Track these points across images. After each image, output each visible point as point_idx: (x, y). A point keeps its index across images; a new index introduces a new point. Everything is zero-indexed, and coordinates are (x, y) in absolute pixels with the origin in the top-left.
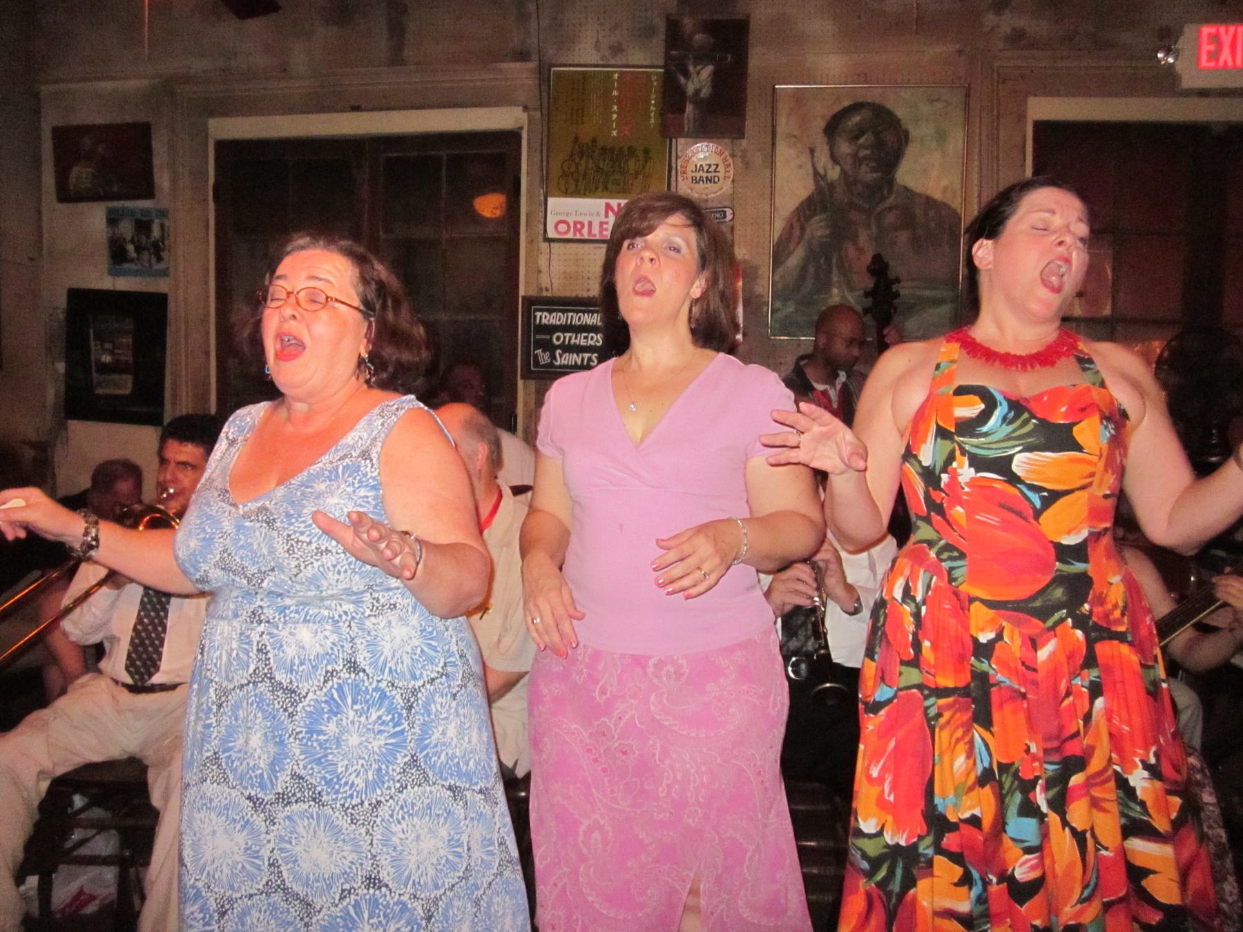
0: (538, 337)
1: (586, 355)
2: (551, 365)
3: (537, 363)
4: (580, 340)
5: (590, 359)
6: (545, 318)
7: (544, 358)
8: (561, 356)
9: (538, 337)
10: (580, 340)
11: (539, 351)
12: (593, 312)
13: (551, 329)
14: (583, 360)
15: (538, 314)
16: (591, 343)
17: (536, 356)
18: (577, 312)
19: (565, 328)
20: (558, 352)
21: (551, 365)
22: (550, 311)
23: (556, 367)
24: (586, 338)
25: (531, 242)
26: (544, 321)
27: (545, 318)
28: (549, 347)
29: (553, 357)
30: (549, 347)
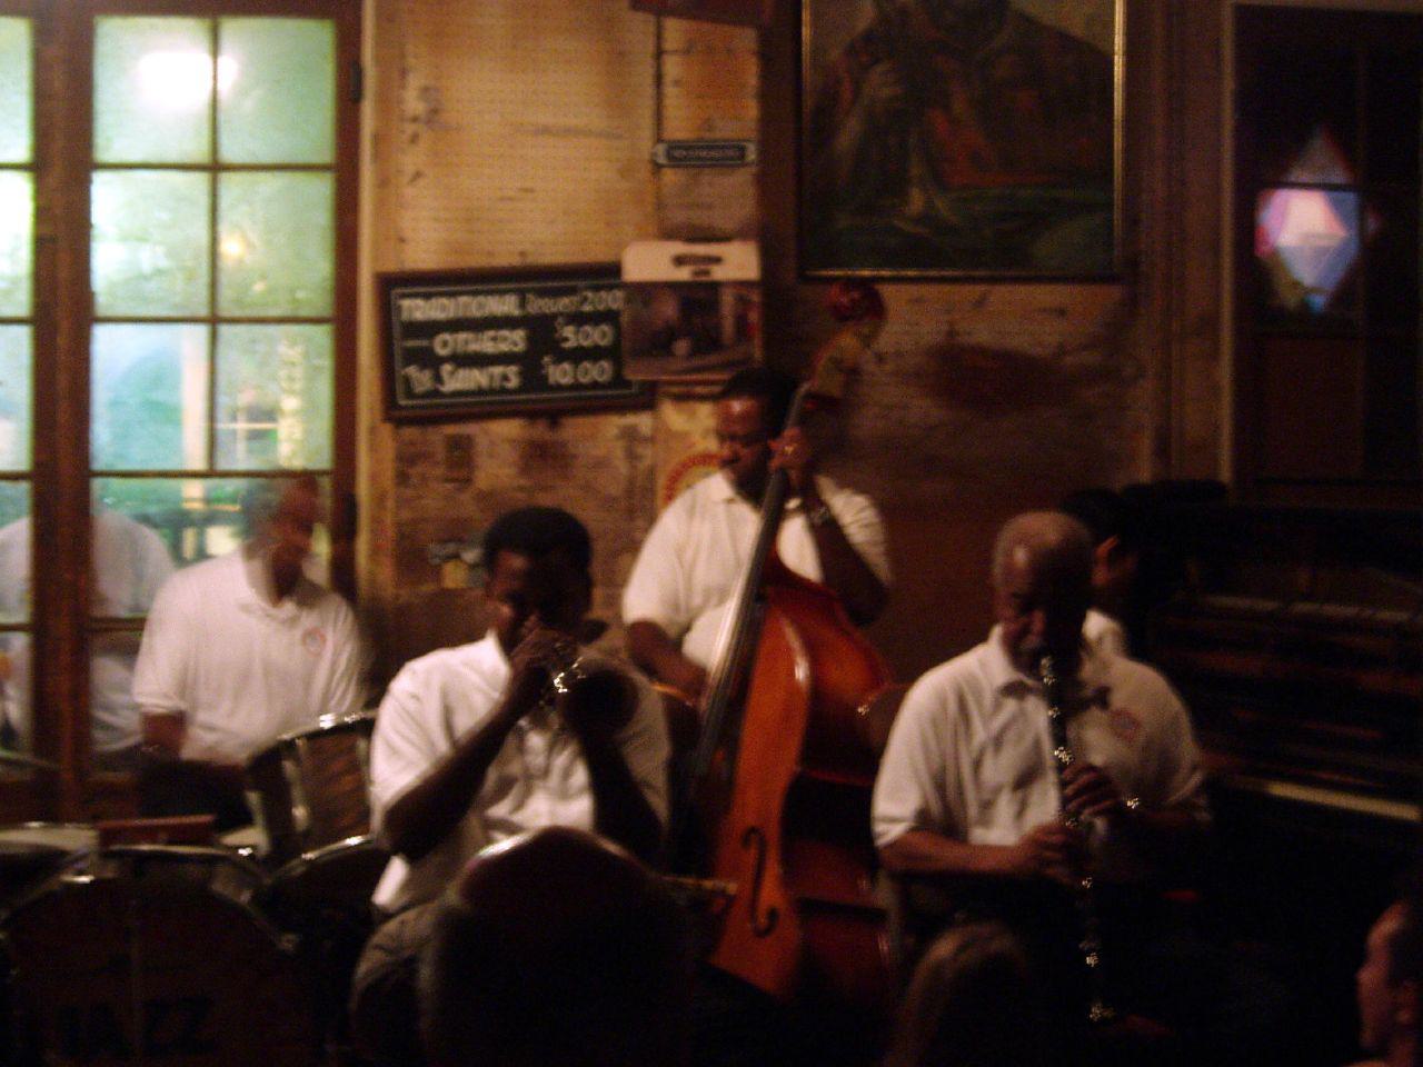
0: (411, 343)
1: (498, 370)
2: (435, 393)
3: (410, 394)
4: (485, 344)
5: (505, 378)
6: (417, 309)
7: (421, 379)
8: (452, 373)
9: (411, 343)
10: (485, 344)
11: (412, 371)
12: (502, 293)
13: (431, 328)
14: (491, 377)
15: (406, 303)
16: (504, 347)
17: (407, 380)
18: (475, 293)
19: (456, 325)
20: (447, 368)
21: (435, 393)
22: (427, 296)
23: (443, 395)
24: (494, 339)
25: (383, 183)
26: (419, 316)
27: (417, 309)
28: (430, 361)
29: (438, 378)
30: (430, 361)
